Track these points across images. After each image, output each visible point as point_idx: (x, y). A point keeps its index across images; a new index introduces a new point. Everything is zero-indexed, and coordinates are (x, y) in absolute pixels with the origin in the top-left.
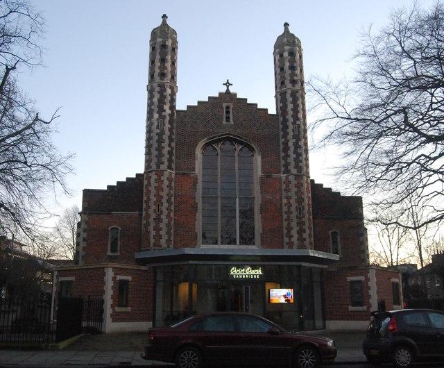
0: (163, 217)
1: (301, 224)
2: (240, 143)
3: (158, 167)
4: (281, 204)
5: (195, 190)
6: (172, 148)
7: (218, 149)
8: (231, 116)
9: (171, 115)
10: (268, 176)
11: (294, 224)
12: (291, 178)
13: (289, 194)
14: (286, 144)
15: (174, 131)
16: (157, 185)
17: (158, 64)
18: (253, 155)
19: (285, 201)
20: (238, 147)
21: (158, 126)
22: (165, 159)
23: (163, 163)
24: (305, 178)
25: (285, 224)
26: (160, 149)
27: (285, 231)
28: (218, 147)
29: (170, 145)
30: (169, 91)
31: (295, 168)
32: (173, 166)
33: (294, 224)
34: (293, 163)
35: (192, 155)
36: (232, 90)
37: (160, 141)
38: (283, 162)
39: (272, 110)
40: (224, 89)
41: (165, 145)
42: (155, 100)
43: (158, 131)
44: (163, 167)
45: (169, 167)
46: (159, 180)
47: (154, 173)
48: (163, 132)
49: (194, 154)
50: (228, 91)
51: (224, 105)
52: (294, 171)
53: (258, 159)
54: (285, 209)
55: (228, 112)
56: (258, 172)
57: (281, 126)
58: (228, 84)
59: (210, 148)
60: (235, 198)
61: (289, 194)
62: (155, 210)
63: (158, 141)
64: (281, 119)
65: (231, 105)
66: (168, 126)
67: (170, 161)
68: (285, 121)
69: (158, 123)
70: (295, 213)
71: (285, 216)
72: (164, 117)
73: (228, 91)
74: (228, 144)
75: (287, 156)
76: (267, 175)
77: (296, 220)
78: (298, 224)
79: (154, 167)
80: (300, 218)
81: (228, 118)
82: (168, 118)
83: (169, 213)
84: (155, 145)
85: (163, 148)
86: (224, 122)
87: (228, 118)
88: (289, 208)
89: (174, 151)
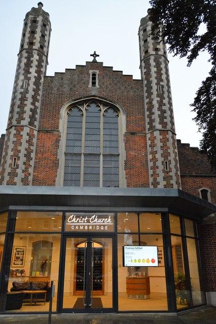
0: (19, 171)
2: (105, 104)
3: (19, 122)
4: (147, 161)
5: (58, 146)
6: (36, 107)
7: (83, 110)
9: (38, 79)
10: (133, 134)
12: (156, 134)
14: (150, 103)
15: (40, 93)
16: (15, 139)
17: (28, 35)
18: (118, 116)
19: (150, 157)
20: (103, 109)
21: (22, 87)
23: (23, 119)
24: (170, 133)
26: (22, 106)
29: (33, 104)
30: (36, 57)
31: (160, 123)
32: (36, 123)
34: (158, 120)
36: (98, 59)
37: (23, 99)
38: (147, 120)
39: (137, 76)
40: (91, 59)
42: (23, 65)
44: (23, 123)
46: (18, 135)
47: (13, 128)
48: (27, 91)
49: (59, 113)
50: (95, 61)
51: (91, 72)
52: (159, 127)
53: (122, 118)
54: (151, 164)
58: (95, 55)
59: (75, 110)
60: (99, 155)
61: (155, 149)
62: (10, 165)
63: (20, 99)
66: (32, 87)
67: (32, 118)
68: (149, 83)
69: (23, 83)
70: (161, 167)
71: (151, 172)
73: (95, 61)
74: (93, 106)
75: (152, 113)
76: (131, 133)
77: (162, 175)
78: (164, 179)
79: (14, 123)
80: (167, 172)
82: (33, 80)
83: (27, 169)
84: (18, 103)
85: (26, 105)
88: (155, 163)
89: (38, 111)
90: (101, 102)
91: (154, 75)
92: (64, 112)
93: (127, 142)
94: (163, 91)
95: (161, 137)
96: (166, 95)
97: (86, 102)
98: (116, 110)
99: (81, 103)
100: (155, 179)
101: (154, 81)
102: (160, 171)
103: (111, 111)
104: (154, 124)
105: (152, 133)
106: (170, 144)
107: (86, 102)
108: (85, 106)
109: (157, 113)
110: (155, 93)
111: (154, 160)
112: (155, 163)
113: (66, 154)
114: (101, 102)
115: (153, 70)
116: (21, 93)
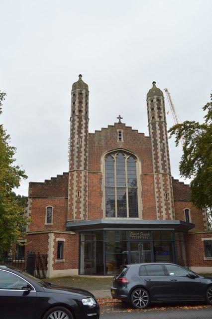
1: (167, 204)
2: (128, 154)
3: (78, 168)
5: (101, 183)
6: (87, 157)
9: (86, 136)
11: (163, 204)
12: (160, 176)
14: (156, 154)
15: (88, 146)
16: (77, 179)
22: (82, 163)
24: (168, 175)
25: (157, 204)
27: (157, 209)
28: (115, 156)
29: (85, 155)
30: (84, 121)
31: (163, 169)
33: (163, 204)
34: (161, 167)
35: (98, 162)
41: (82, 154)
43: (78, 146)
44: (82, 168)
45: (85, 168)
48: (81, 147)
49: (100, 160)
52: (162, 171)
53: (139, 164)
54: (157, 195)
56: (139, 171)
57: (153, 144)
64: (153, 139)
66: (83, 143)
68: (155, 141)
70: (163, 197)
71: (157, 200)
72: (81, 137)
75: (157, 162)
76: (144, 175)
77: (164, 202)
82: (84, 138)
90: (125, 152)
91: (159, 136)
92: (103, 159)
93: (142, 180)
94: (164, 147)
95: (163, 178)
96: (166, 150)
97: (116, 152)
99: (113, 153)
100: (160, 205)
101: (159, 140)
102: (162, 199)
104: (159, 169)
105: (157, 175)
106: (168, 183)
107: (116, 152)
108: (116, 155)
109: (161, 162)
110: (159, 148)
111: (159, 192)
113: (106, 187)
114: (125, 152)
115: (158, 132)
116: (77, 148)
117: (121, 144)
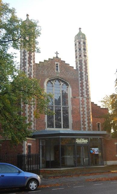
2: (63, 81)
8: (59, 68)
13: (84, 106)
18: (68, 88)
19: (81, 109)
20: (62, 83)
28: (53, 82)
36: (59, 56)
40: (55, 56)
51: (56, 63)
54: (82, 113)
55: (57, 67)
58: (57, 53)
65: (59, 64)
71: (82, 116)
73: (57, 57)
81: (57, 69)
86: (56, 71)
87: (57, 69)
88: (84, 112)
90: (61, 80)
92: (45, 84)
97: (54, 79)
98: (67, 85)
99: (53, 80)
103: (65, 85)
112: (84, 112)
117: (58, 73)
